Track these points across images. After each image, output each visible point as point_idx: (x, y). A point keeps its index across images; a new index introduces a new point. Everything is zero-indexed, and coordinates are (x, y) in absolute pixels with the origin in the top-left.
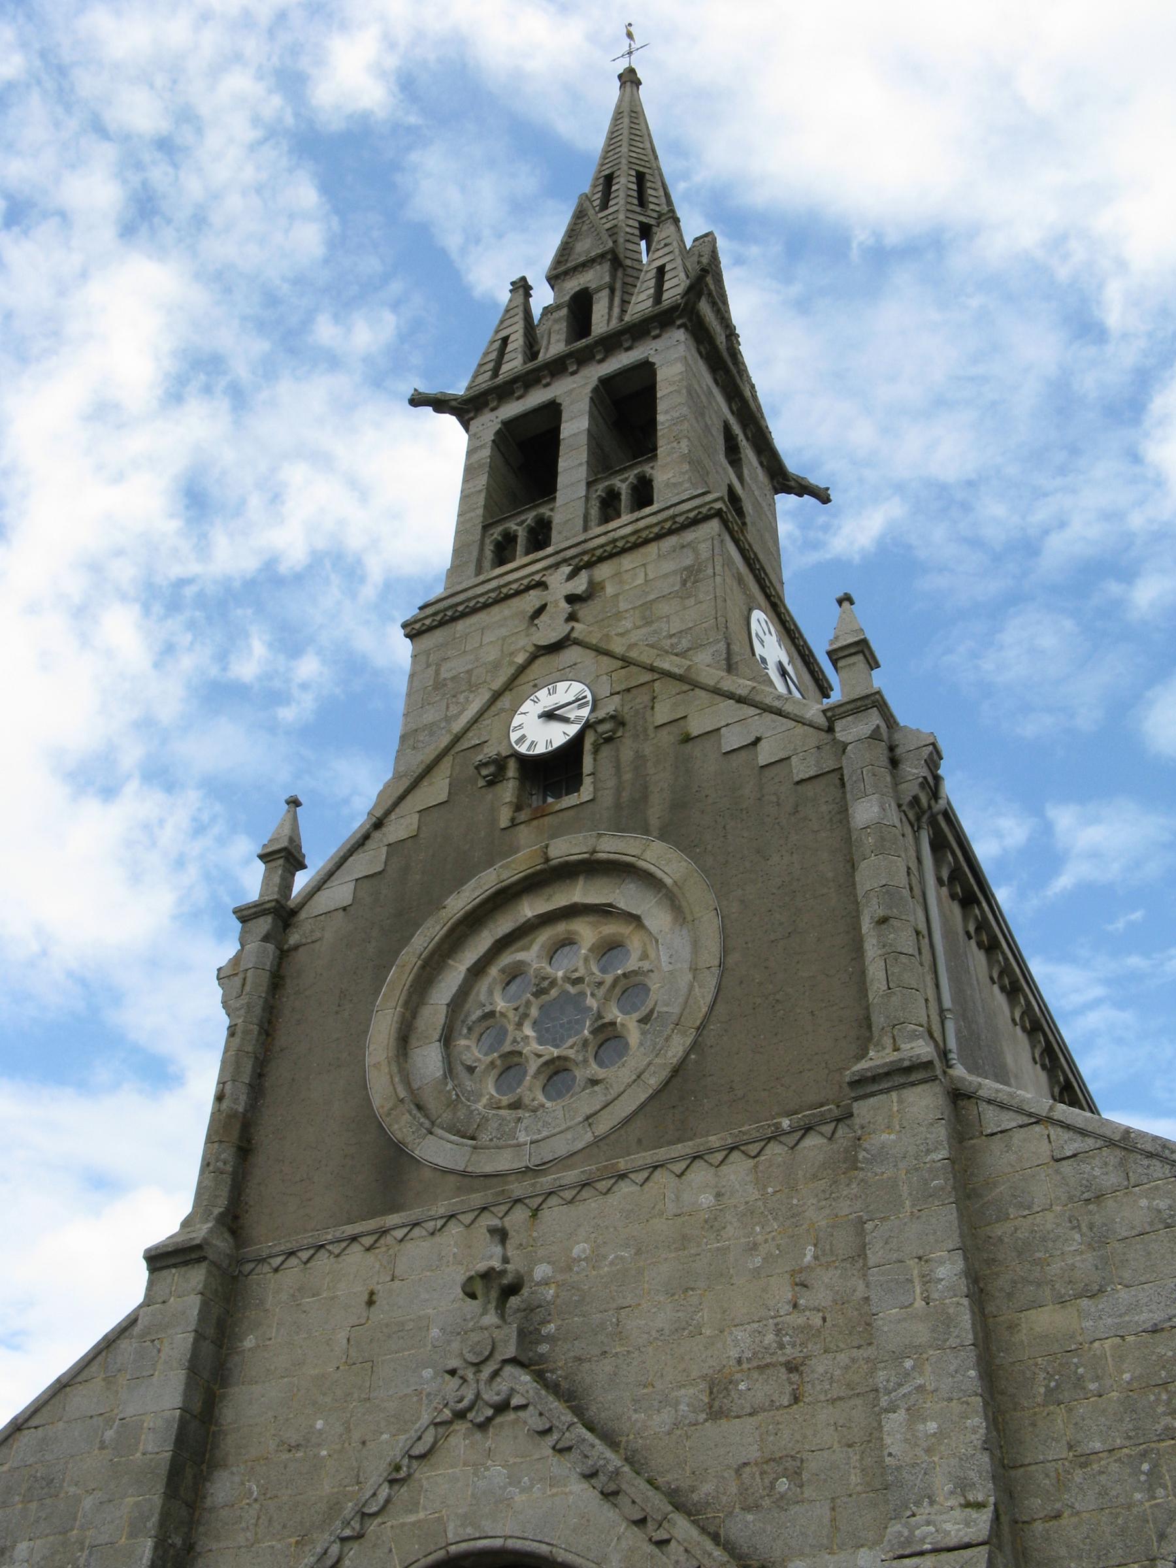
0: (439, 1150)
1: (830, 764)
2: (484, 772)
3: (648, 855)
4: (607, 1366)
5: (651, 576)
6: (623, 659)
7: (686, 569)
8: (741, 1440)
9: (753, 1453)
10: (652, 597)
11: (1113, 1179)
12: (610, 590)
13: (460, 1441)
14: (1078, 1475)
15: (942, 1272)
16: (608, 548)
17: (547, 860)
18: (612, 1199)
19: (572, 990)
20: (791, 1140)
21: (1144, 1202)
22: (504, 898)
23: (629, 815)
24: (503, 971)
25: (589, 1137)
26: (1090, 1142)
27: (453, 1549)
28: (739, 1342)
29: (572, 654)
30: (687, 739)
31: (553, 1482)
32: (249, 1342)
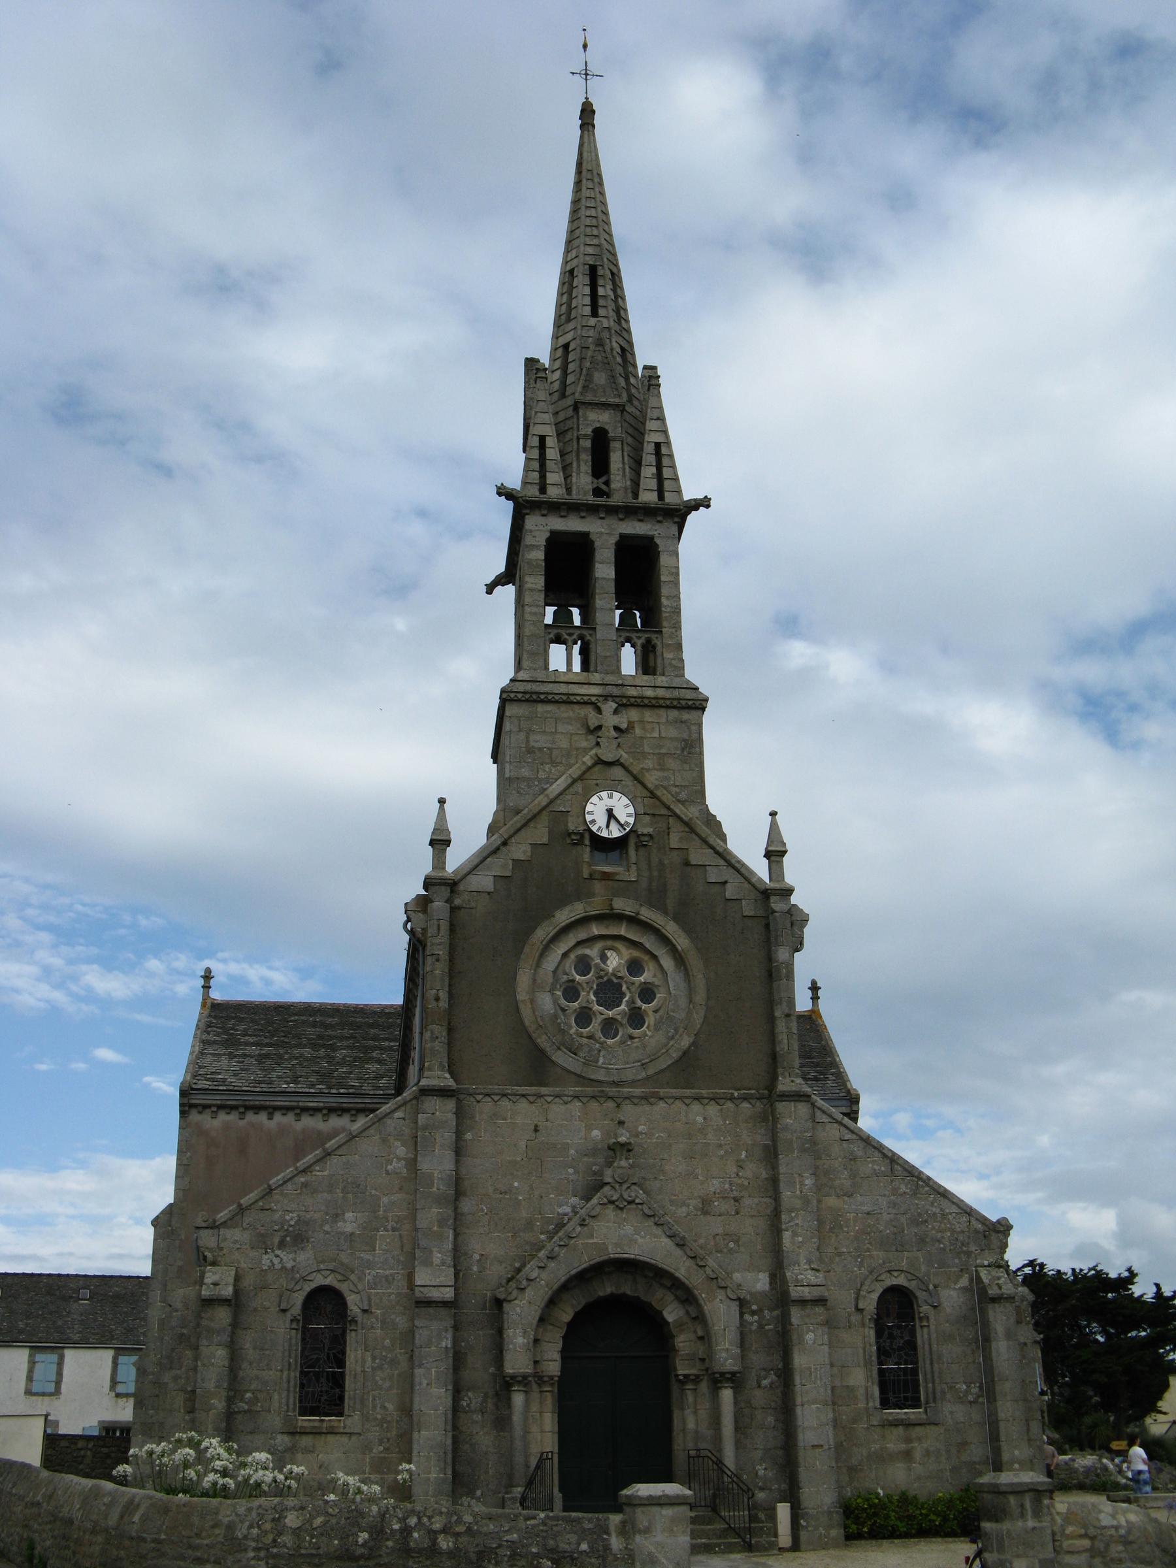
0: (562, 1058)
1: (761, 913)
2: (574, 837)
3: (668, 928)
4: (657, 1184)
6: (651, 792)
7: (684, 740)
8: (716, 1225)
9: (720, 1231)
10: (663, 751)
11: (860, 1153)
12: (638, 731)
13: (610, 1211)
14: (837, 1259)
15: (807, 1182)
17: (612, 909)
18: (656, 1108)
19: (615, 980)
20: (737, 1102)
22: (585, 921)
23: (656, 898)
25: (644, 1074)
26: (854, 1137)
28: (715, 1185)
29: (617, 772)
30: (687, 864)
31: (656, 1236)
32: (468, 1136)
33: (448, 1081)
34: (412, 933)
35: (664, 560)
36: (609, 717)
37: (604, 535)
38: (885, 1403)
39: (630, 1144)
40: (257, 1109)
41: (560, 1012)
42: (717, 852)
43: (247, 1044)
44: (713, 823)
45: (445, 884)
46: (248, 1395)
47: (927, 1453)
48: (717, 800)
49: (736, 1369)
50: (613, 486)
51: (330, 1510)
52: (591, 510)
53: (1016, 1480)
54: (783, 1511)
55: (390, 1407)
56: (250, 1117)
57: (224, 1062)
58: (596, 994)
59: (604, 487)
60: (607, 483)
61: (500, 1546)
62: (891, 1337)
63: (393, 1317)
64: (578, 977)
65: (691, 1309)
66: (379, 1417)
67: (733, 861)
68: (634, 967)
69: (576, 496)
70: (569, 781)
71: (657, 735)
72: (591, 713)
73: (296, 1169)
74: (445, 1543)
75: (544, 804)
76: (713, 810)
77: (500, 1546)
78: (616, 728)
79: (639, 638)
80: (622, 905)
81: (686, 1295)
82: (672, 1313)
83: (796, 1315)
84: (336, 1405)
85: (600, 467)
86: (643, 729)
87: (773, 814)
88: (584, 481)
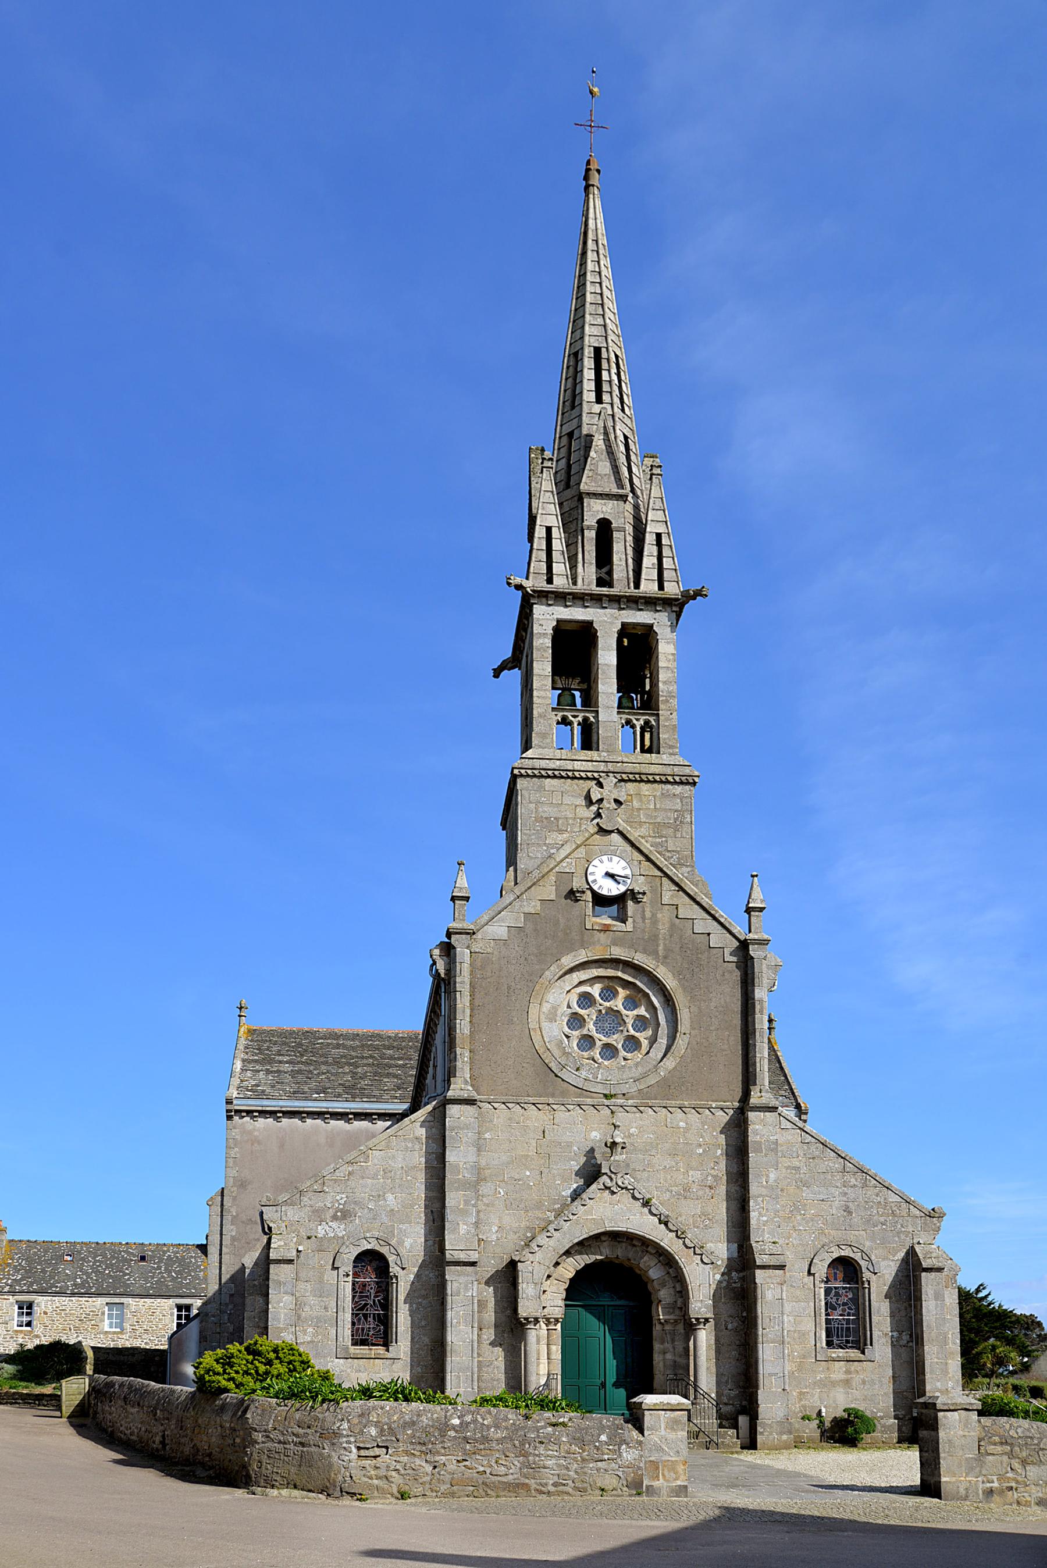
5: (658, 806)
23: (649, 946)
36: (610, 790)
37: (608, 624)
38: (829, 1344)
47: (864, 1382)
50: (615, 576)
52: (597, 600)
60: (610, 573)
62: (837, 1294)
69: (580, 587)
71: (652, 807)
78: (616, 801)
81: (667, 1260)
85: (604, 558)
86: (641, 801)
88: (588, 575)
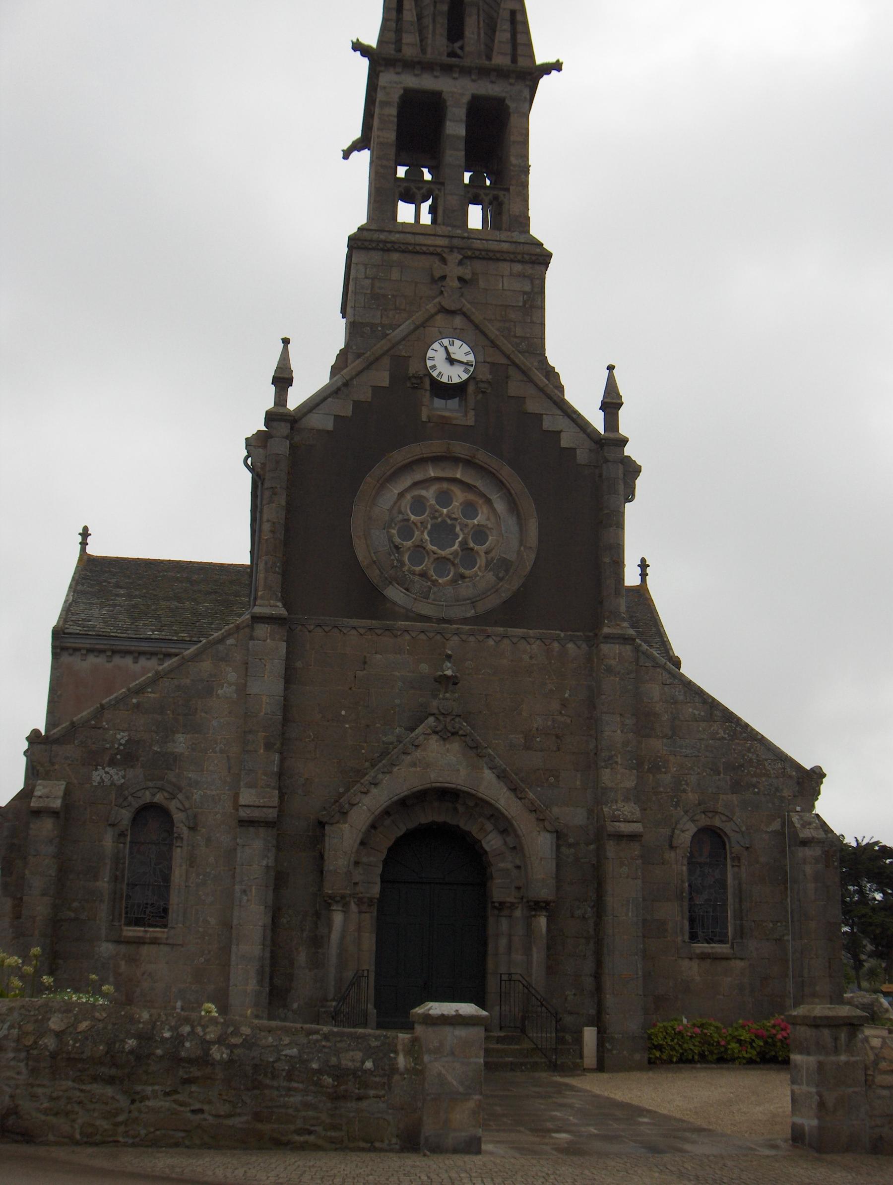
0: (395, 593)
2: (414, 381)
7: (525, 293)
11: (681, 698)
16: (483, 253)
19: (449, 522)
21: (690, 710)
22: (422, 461)
24: (413, 497)
27: (434, 785)
29: (458, 321)
33: (282, 611)
34: (251, 469)
35: (514, 120)
37: (457, 91)
38: (693, 937)
39: (456, 676)
40: (125, 653)
41: (395, 550)
42: (555, 403)
43: (117, 595)
44: (551, 375)
45: (285, 421)
46: (75, 904)
48: (556, 352)
49: (550, 898)
50: (467, 49)
51: (97, 1014)
52: (447, 69)
53: (831, 1014)
54: (590, 1034)
55: (213, 921)
56: (117, 660)
57: (95, 612)
58: (429, 534)
59: (459, 52)
60: (462, 48)
61: (278, 1060)
63: (218, 835)
64: (413, 517)
65: (510, 840)
66: (201, 930)
67: (569, 411)
68: (470, 509)
69: (429, 56)
70: (412, 327)
72: (437, 263)
73: (129, 690)
74: (218, 1053)
75: (385, 348)
76: (551, 362)
77: (278, 1060)
78: (460, 279)
79: (487, 195)
80: (460, 449)
81: (505, 827)
82: (492, 842)
83: (611, 849)
84: (163, 917)
85: (455, 32)
87: (611, 368)
88: (438, 44)
